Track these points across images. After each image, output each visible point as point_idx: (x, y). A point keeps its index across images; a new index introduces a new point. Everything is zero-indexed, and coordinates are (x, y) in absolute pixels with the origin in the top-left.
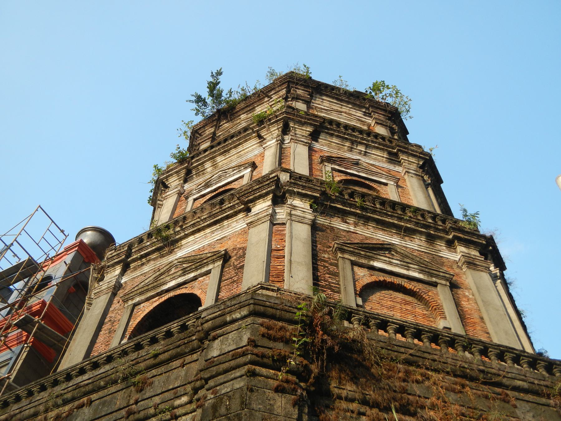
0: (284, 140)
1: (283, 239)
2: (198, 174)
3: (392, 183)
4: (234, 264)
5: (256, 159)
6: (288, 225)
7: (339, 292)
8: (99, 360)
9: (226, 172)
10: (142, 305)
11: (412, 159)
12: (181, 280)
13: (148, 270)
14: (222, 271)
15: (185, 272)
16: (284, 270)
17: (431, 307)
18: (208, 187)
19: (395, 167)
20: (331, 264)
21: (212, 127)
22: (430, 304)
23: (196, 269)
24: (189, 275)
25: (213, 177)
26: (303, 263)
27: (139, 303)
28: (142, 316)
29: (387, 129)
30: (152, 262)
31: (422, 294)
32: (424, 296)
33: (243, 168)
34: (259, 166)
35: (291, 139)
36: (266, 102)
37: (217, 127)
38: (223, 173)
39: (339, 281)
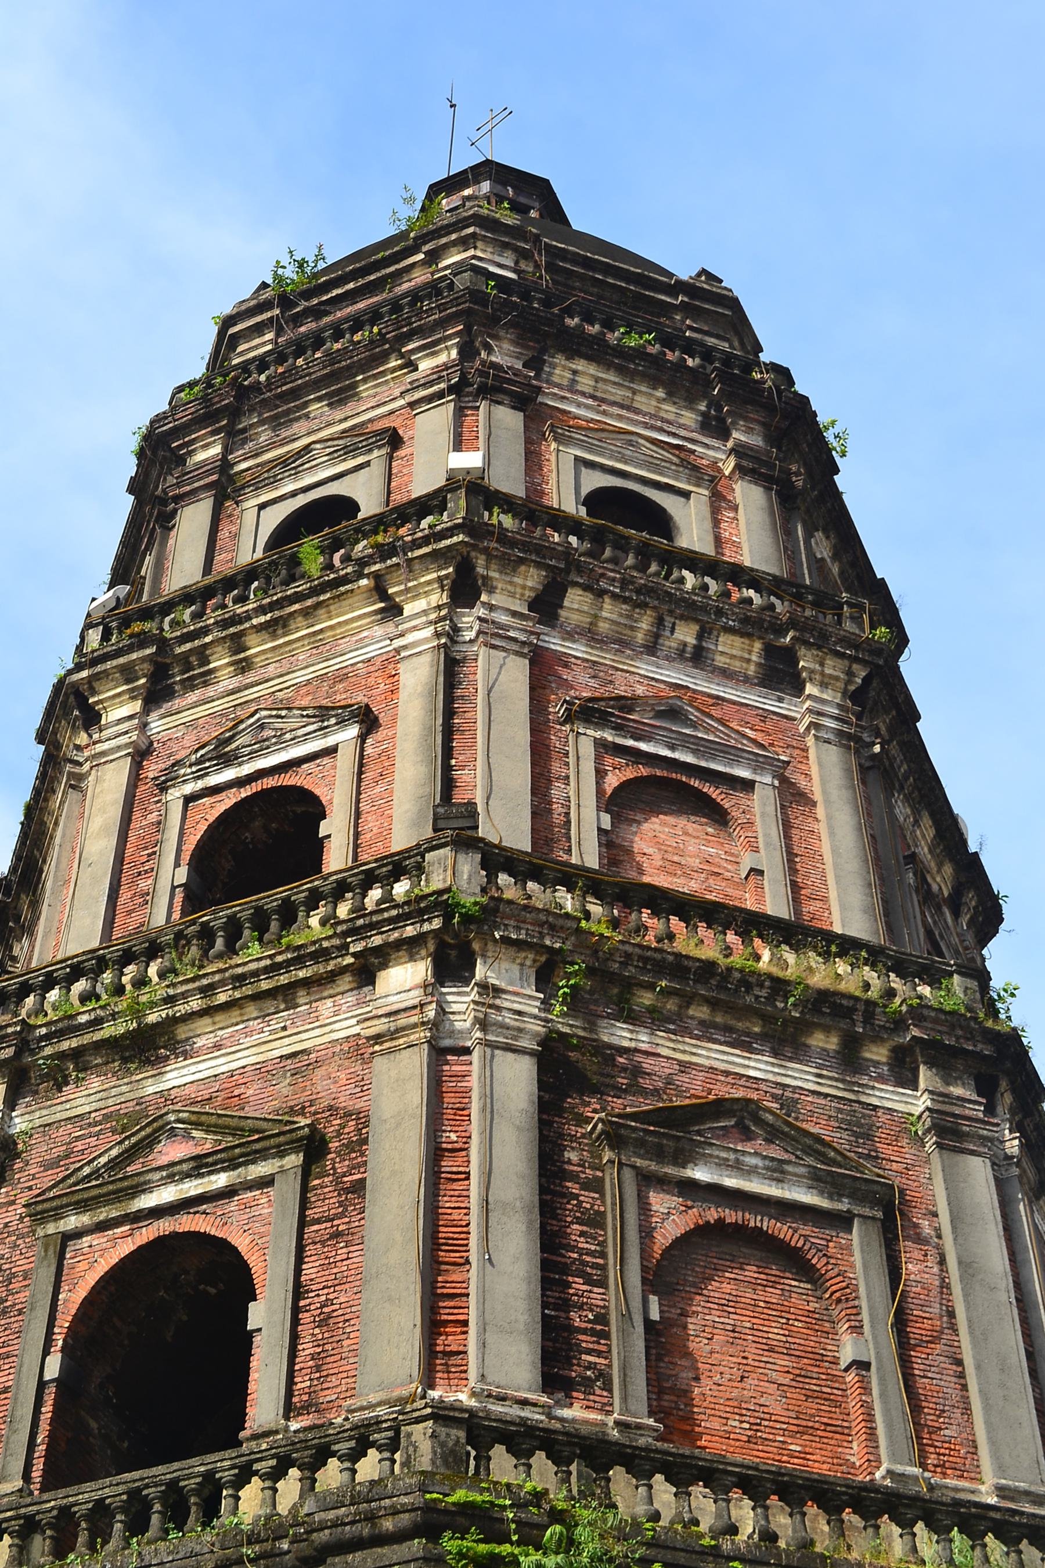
0: (456, 630)
1: (463, 1109)
2: (190, 685)
3: (768, 779)
4: (334, 1168)
5: (371, 681)
6: (475, 1056)
7: (603, 1283)
8: (38, 1512)
9: (282, 717)
10: (86, 1240)
11: (833, 667)
12: (192, 1188)
13: (87, 1109)
14: (305, 1189)
15: (200, 1165)
16: (468, 1225)
17: (829, 1292)
18: (227, 760)
19: (780, 700)
20: (587, 1186)
21: (213, 433)
22: (828, 1284)
23: (232, 1165)
24: (213, 1178)
25: (242, 727)
26: (518, 1204)
27: (78, 1234)
28: (92, 1278)
29: (768, 489)
30: (95, 1083)
31: (809, 1256)
32: (814, 1261)
33: (333, 721)
34: (383, 718)
35: (480, 632)
36: (394, 370)
37: (234, 437)
38: (271, 716)
39: (603, 1244)
